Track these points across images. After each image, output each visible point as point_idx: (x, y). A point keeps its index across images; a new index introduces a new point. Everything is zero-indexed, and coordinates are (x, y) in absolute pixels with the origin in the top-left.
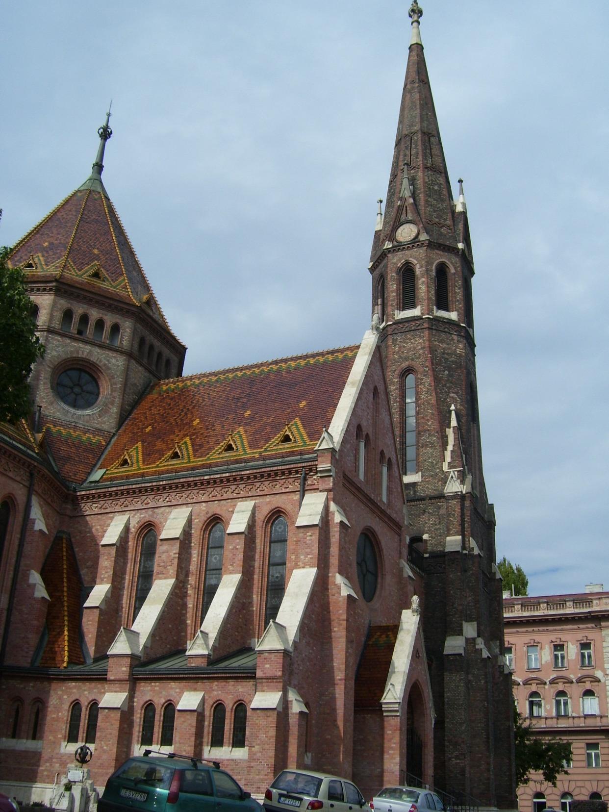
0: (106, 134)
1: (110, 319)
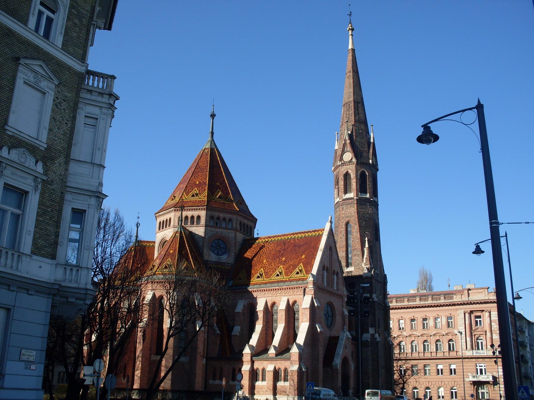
0: (213, 116)
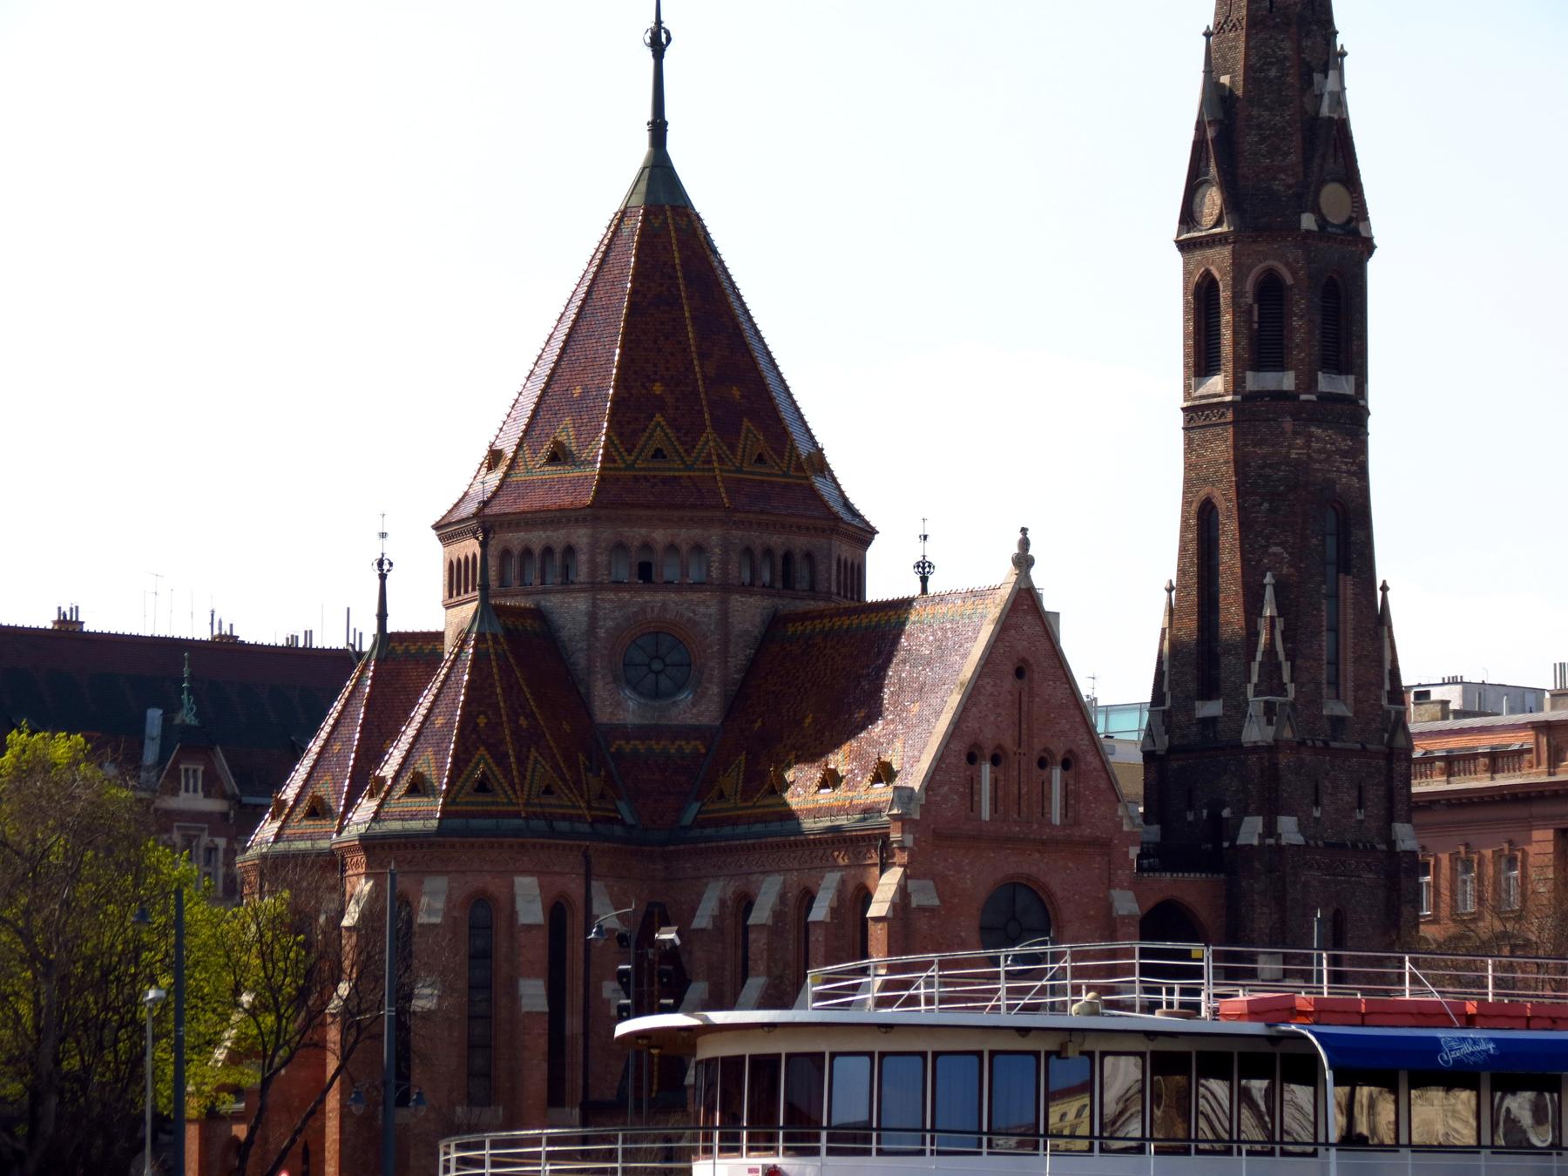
0: (658, 43)
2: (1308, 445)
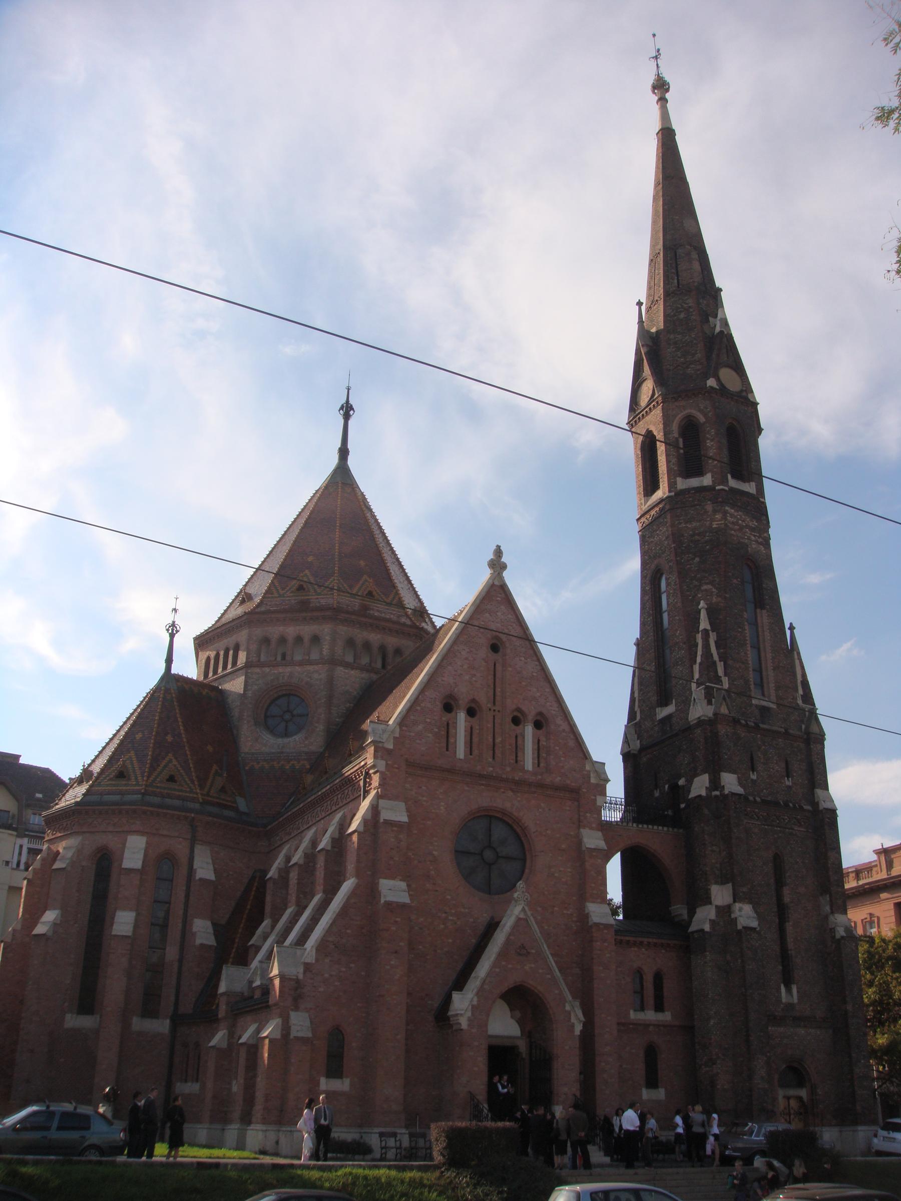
0: (347, 410)
1: (307, 630)
2: (724, 517)
